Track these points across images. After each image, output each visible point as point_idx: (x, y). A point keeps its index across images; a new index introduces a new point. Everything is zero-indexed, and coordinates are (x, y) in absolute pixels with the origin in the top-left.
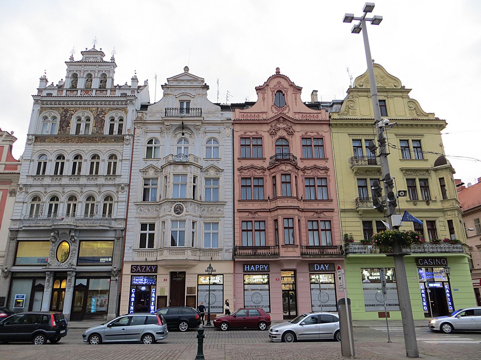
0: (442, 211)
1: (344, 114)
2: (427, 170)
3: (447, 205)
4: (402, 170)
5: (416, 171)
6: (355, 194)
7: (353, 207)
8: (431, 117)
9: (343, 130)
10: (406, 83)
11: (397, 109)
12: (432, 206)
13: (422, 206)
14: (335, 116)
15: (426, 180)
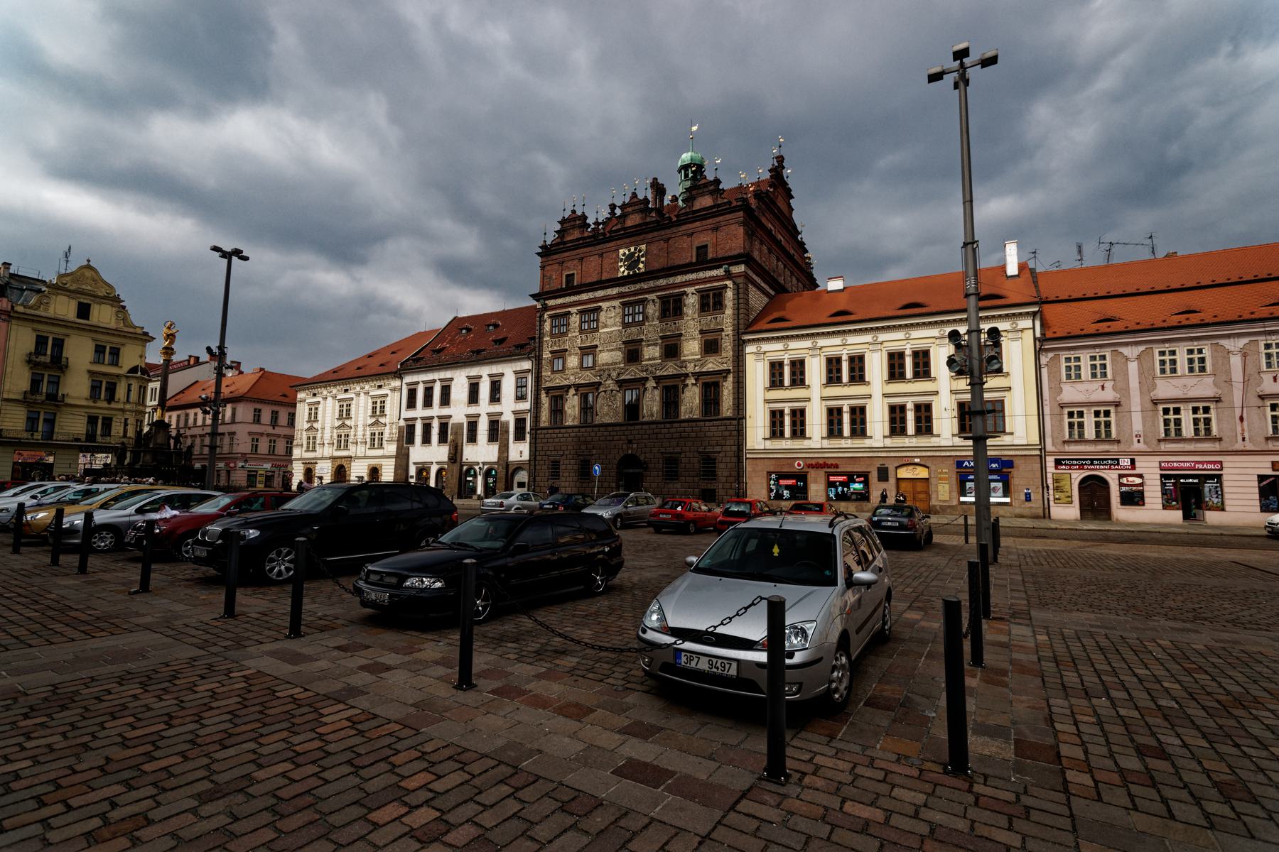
0: (123, 410)
1: (30, 308)
2: (118, 376)
3: (128, 406)
4: (89, 371)
5: (105, 374)
6: (24, 385)
7: (20, 397)
8: (139, 331)
9: (26, 323)
10: (121, 291)
11: (102, 315)
12: (113, 405)
13: (105, 405)
14: (20, 309)
15: (115, 384)
